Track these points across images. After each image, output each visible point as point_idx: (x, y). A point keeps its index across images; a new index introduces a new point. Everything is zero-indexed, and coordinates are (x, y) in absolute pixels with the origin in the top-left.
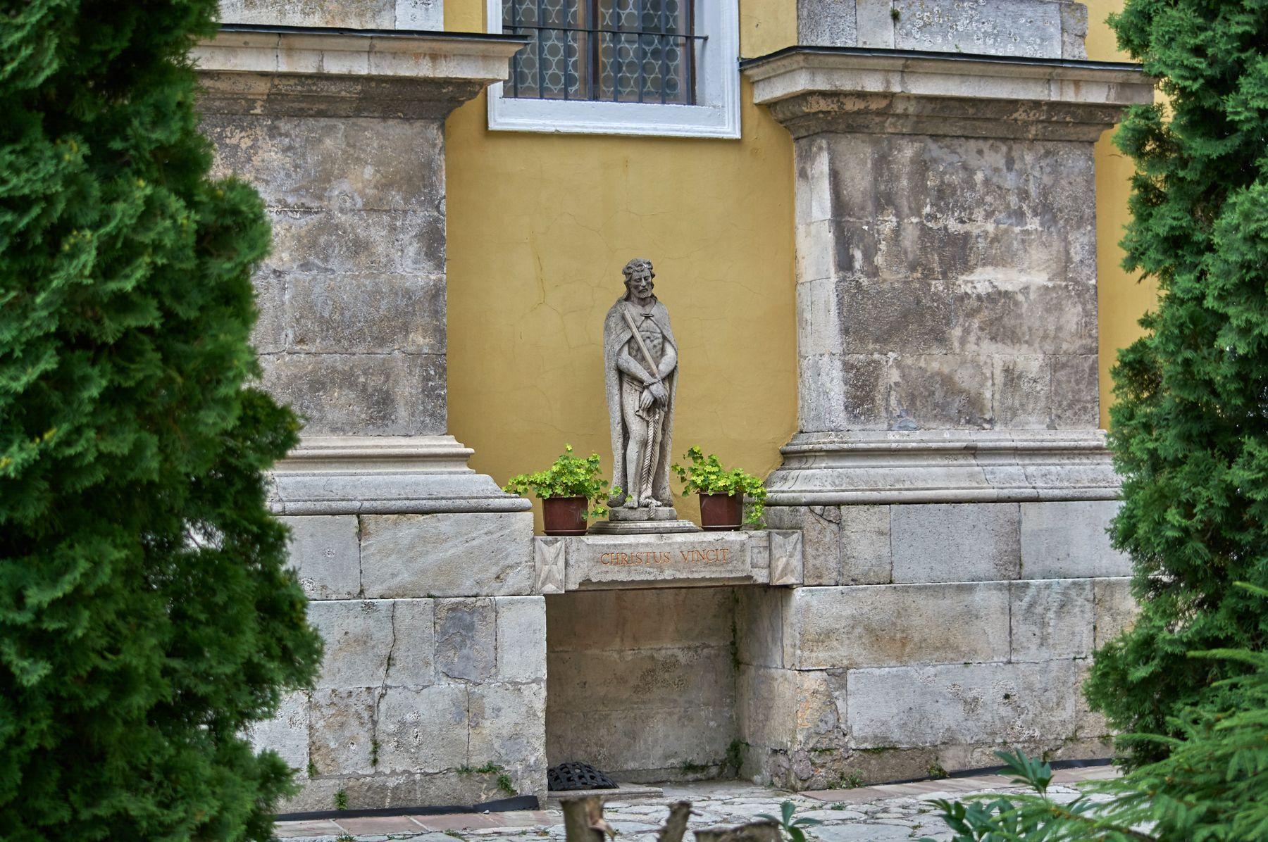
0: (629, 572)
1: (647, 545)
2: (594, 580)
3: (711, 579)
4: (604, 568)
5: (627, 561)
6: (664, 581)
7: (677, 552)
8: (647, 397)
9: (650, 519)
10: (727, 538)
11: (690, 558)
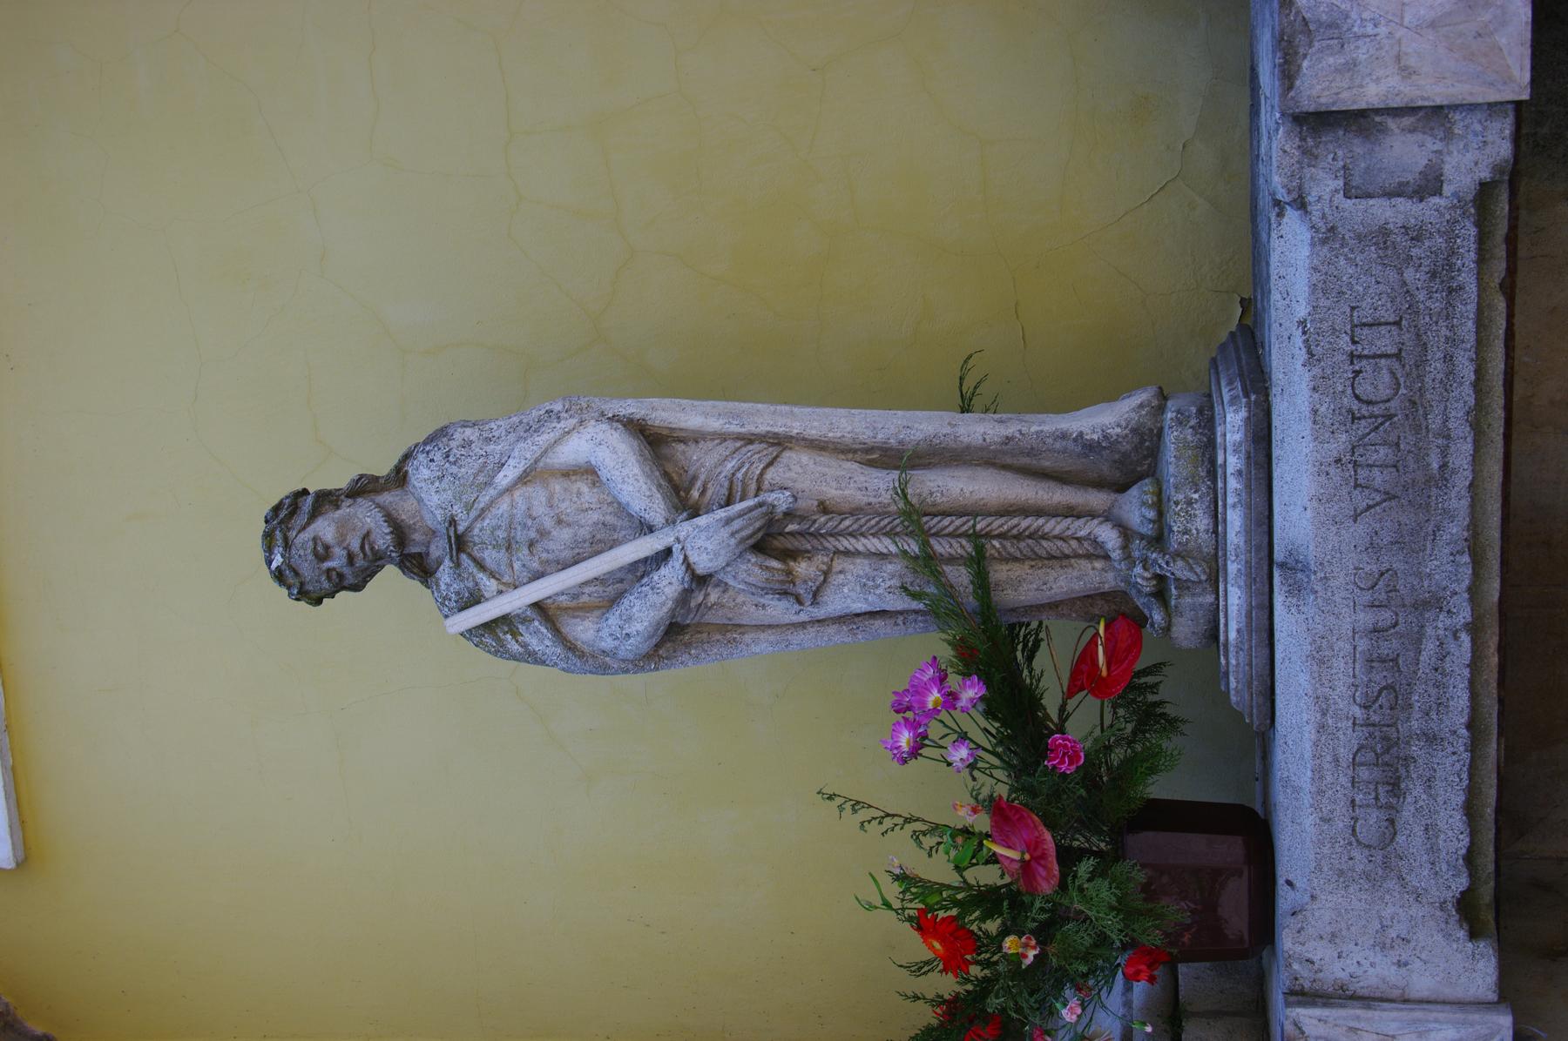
0: (1431, 739)
1: (1319, 660)
2: (1462, 882)
3: (1479, 385)
4: (1411, 839)
5: (1385, 763)
6: (1474, 592)
7: (1360, 530)
8: (753, 570)
9: (1215, 578)
10: (1302, 311)
11: (1378, 478)
